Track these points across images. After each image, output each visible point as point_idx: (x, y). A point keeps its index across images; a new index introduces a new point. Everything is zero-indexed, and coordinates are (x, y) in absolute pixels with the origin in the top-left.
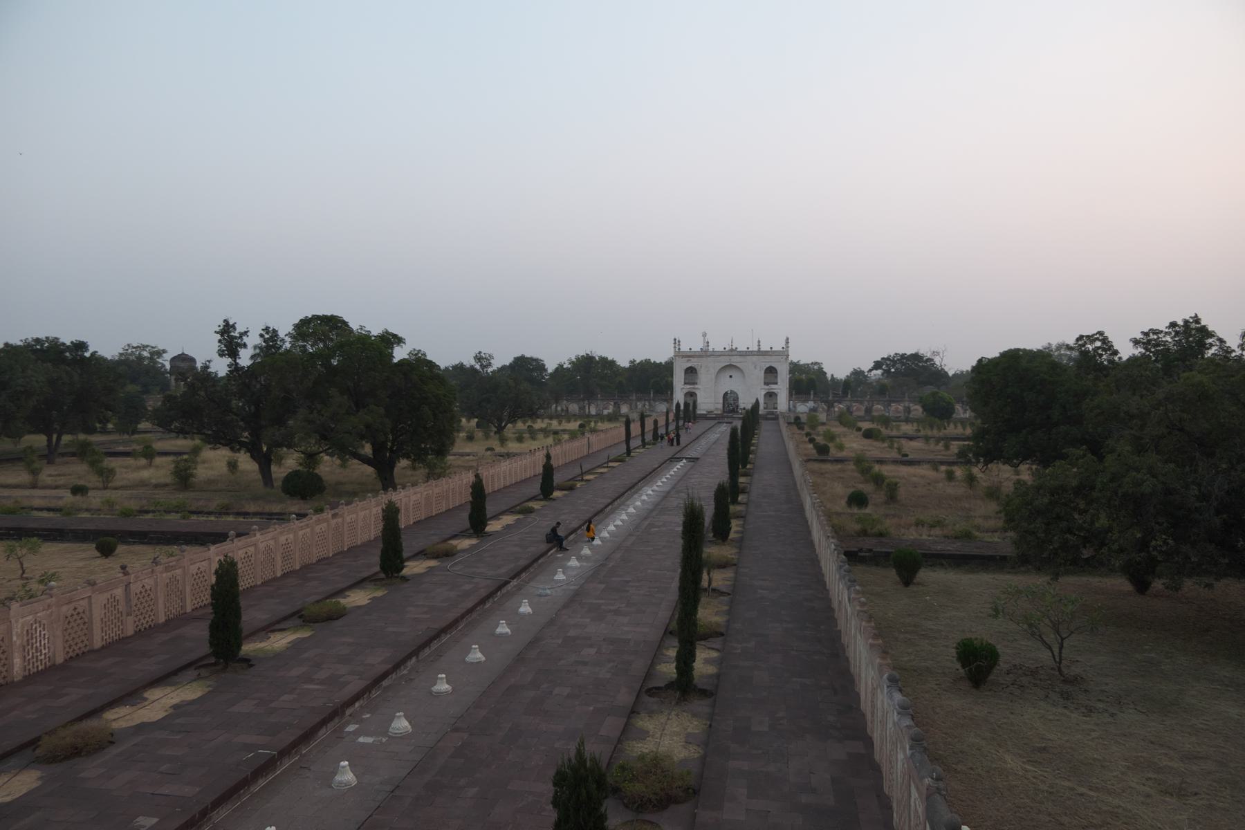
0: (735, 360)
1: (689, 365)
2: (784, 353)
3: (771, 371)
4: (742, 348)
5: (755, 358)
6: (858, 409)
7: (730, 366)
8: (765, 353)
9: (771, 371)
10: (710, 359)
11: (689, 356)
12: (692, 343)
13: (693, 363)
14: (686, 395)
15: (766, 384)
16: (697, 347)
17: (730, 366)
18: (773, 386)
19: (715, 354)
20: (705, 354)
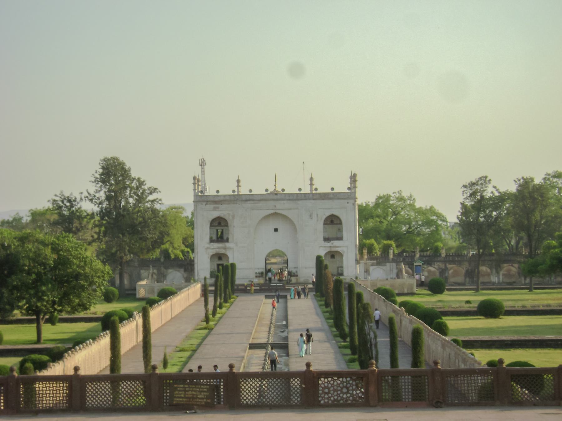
0: (282, 207)
1: (216, 214)
2: (350, 196)
3: (333, 221)
4: (292, 189)
5: (310, 203)
6: (456, 274)
7: (275, 215)
8: (324, 196)
9: (333, 221)
10: (249, 205)
11: (217, 201)
12: (219, 184)
13: (222, 212)
14: (213, 257)
15: (326, 239)
16: (227, 190)
17: (275, 215)
18: (336, 243)
19: (251, 199)
20: (235, 199)
